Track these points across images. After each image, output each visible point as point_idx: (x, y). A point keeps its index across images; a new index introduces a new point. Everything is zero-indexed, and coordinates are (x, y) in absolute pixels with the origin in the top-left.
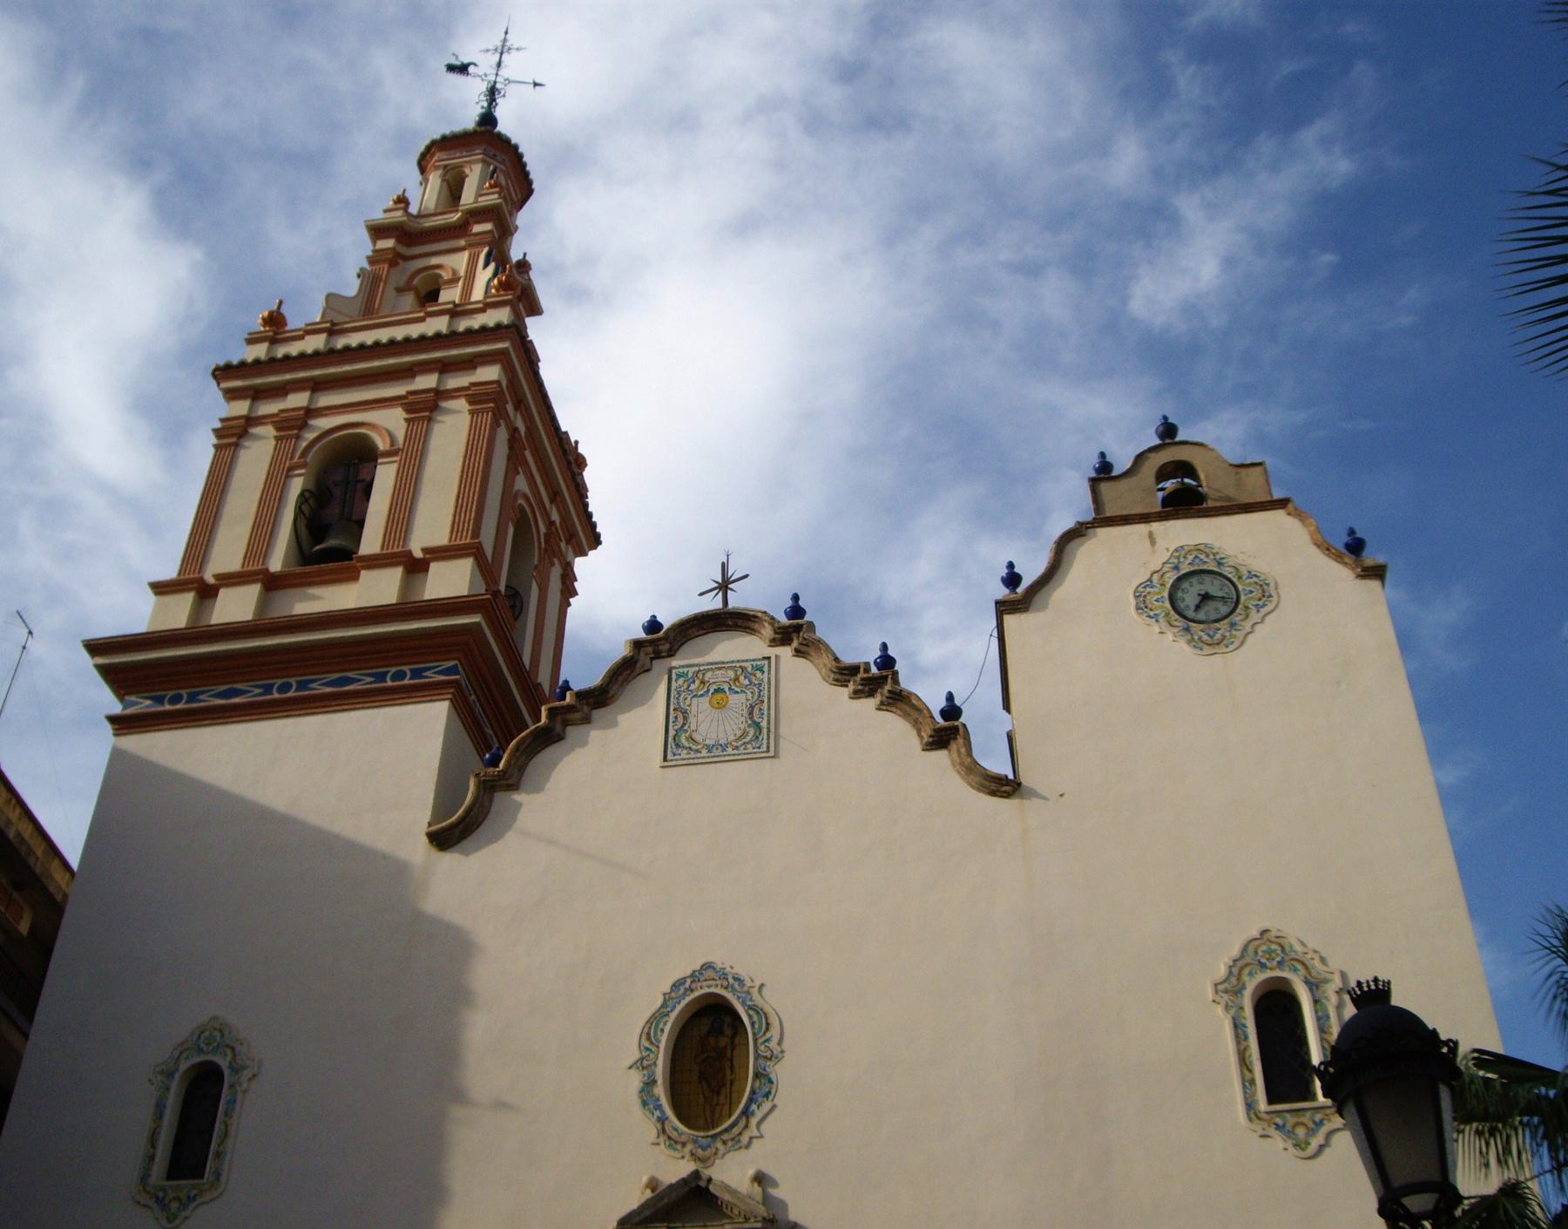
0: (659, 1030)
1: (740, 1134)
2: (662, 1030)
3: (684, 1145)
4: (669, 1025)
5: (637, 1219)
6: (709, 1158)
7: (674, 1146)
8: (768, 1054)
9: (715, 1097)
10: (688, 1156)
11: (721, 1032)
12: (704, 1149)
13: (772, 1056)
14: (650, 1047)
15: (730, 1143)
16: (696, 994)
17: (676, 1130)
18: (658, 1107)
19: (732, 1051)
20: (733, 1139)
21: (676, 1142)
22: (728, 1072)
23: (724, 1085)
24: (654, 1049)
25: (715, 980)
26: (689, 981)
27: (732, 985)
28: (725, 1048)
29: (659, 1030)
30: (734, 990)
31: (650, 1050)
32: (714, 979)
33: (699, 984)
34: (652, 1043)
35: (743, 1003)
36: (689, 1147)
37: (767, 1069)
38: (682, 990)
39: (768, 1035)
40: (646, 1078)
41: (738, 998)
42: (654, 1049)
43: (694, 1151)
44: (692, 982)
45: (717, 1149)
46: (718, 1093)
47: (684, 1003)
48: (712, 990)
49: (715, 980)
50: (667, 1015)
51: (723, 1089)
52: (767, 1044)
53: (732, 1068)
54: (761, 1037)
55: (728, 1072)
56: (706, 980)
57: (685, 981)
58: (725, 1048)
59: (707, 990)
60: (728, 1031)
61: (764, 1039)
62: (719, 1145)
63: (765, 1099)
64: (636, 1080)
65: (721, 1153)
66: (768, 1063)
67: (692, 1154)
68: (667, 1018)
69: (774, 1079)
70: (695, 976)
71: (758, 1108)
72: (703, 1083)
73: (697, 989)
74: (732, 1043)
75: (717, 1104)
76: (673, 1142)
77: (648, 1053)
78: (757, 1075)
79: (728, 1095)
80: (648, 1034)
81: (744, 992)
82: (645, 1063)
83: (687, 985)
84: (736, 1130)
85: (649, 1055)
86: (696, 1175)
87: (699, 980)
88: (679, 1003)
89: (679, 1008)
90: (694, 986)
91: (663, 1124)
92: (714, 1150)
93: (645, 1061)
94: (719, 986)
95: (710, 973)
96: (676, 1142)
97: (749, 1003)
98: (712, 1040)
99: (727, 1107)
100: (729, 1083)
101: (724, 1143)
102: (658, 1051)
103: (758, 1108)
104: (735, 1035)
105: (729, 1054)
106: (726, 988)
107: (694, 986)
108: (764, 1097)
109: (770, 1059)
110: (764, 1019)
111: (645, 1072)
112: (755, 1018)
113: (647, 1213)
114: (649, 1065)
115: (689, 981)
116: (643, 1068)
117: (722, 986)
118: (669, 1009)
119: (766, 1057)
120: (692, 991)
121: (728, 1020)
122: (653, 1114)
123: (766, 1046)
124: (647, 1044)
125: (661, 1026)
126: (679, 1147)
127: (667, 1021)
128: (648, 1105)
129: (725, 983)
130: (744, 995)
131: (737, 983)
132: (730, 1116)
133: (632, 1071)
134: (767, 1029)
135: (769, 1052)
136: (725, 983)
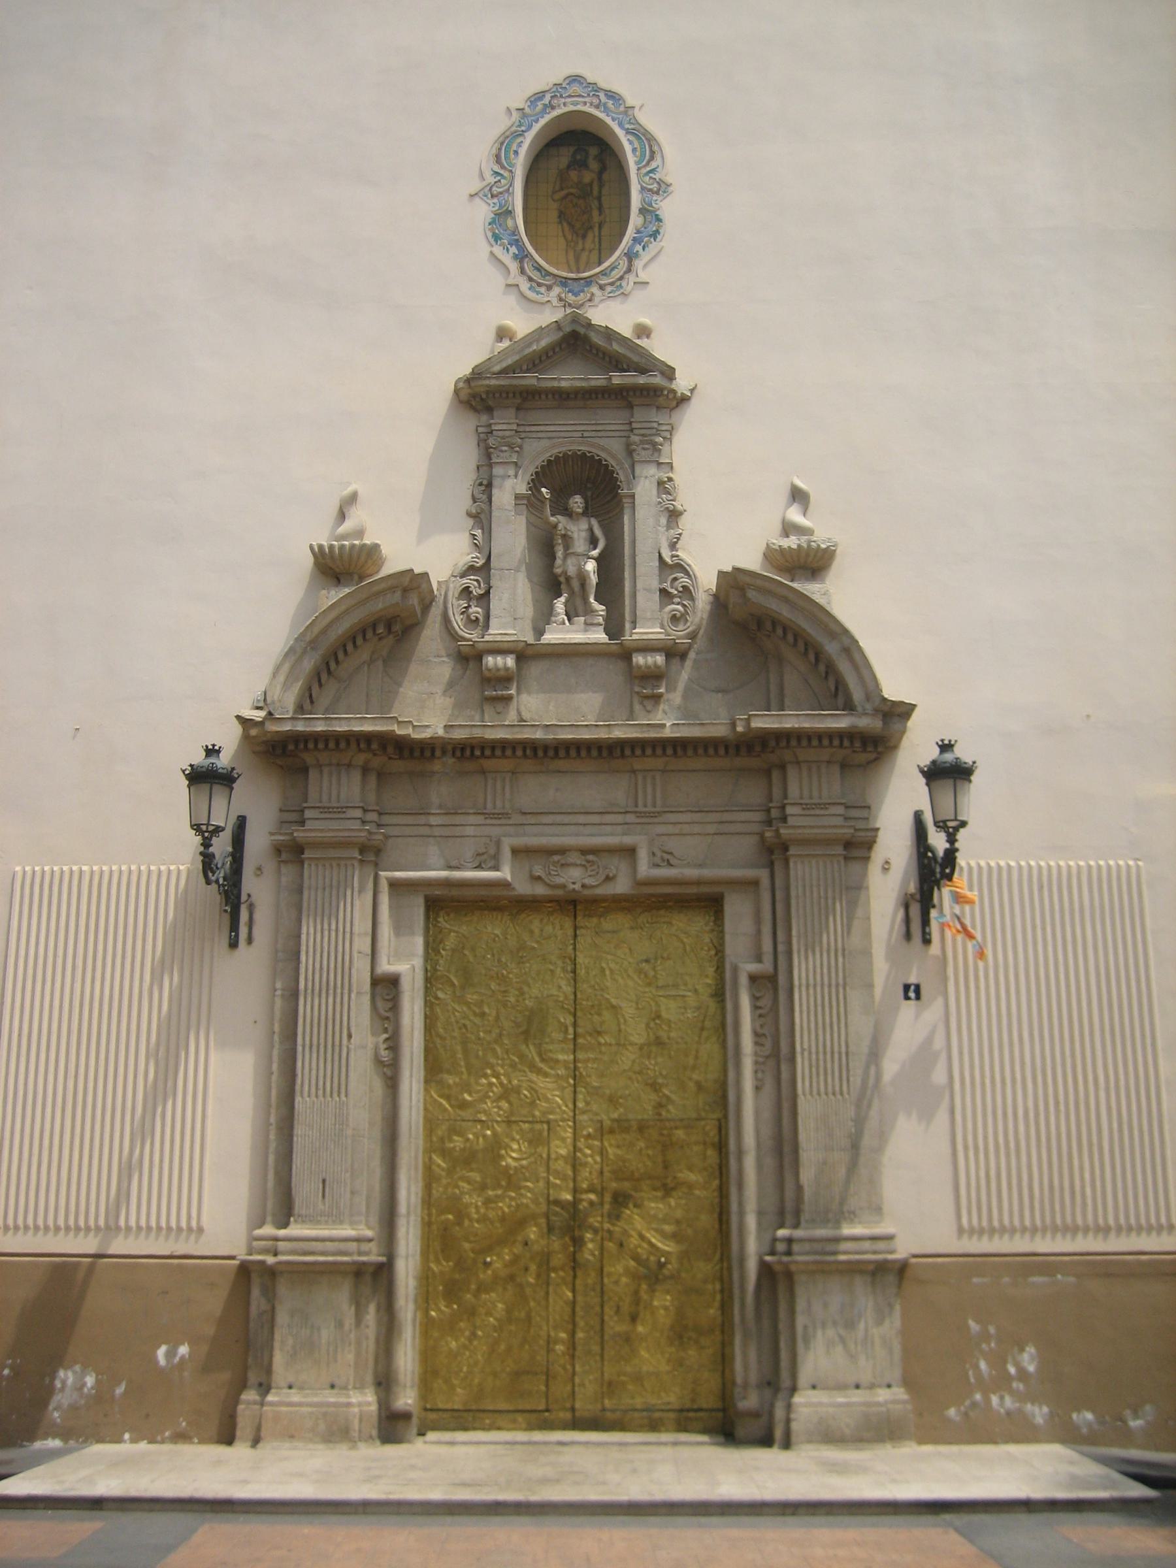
0: (512, 152)
1: (621, 278)
2: (516, 153)
3: (549, 288)
4: (523, 151)
5: (497, 368)
6: (582, 305)
7: (538, 289)
8: (655, 187)
9: (580, 242)
10: (555, 302)
11: (584, 165)
12: (576, 294)
13: (659, 190)
14: (502, 172)
15: (609, 289)
16: (555, 113)
17: (539, 268)
18: (517, 243)
19: (601, 186)
20: (612, 284)
21: (539, 285)
22: (595, 213)
23: (591, 228)
24: (506, 174)
25: (583, 96)
26: (548, 97)
27: (605, 104)
28: (591, 184)
29: (512, 152)
30: (607, 110)
31: (501, 175)
32: (580, 96)
33: (563, 100)
34: (503, 167)
35: (621, 125)
36: (557, 290)
37: (654, 205)
38: (540, 106)
39: (653, 165)
40: (497, 208)
41: (613, 120)
42: (506, 174)
43: (563, 295)
44: (552, 97)
45: (593, 294)
46: (584, 237)
47: (543, 122)
48: (580, 108)
49: (583, 96)
50: (521, 135)
51: (590, 235)
52: (651, 175)
53: (600, 208)
54: (645, 166)
55: (595, 213)
56: (570, 96)
57: (544, 96)
58: (591, 184)
59: (571, 108)
60: (594, 165)
61: (648, 169)
62: (595, 289)
63: (652, 240)
64: (483, 211)
65: (597, 299)
66: (655, 198)
67: (561, 299)
68: (520, 139)
69: (661, 217)
70: (557, 91)
71: (644, 249)
72: (565, 224)
73: (559, 106)
74: (600, 178)
75: (583, 249)
76: (534, 285)
77: (499, 178)
78: (643, 211)
79: (597, 240)
80: (498, 157)
81: (620, 113)
82: (495, 190)
83: (547, 100)
84: (616, 274)
85: (499, 181)
86: (575, 319)
87: (561, 96)
88: (537, 121)
89: (537, 128)
90: (555, 102)
91: (521, 262)
92: (589, 295)
93: (494, 189)
94: (588, 104)
95: (576, 88)
96: (539, 285)
97: (627, 126)
98: (573, 175)
99: (596, 252)
100: (597, 225)
101: (602, 288)
102: (513, 178)
103: (644, 249)
104: (603, 169)
105: (595, 192)
106: (597, 107)
107: (555, 102)
108: (650, 236)
109: (657, 193)
110: (647, 147)
111: (495, 200)
112: (636, 145)
113: (509, 361)
114: (501, 193)
115: (548, 97)
116: (492, 196)
117: (591, 104)
118: (523, 128)
119: (650, 190)
120: (553, 108)
121: (593, 151)
122: (508, 250)
123: (651, 178)
124: (497, 168)
125: (514, 147)
126: (543, 290)
127: (522, 142)
128: (501, 239)
129: (596, 101)
130: (621, 116)
131: (611, 102)
132: (600, 264)
133: (477, 200)
134: (652, 158)
135: (655, 185)
136: (596, 101)
